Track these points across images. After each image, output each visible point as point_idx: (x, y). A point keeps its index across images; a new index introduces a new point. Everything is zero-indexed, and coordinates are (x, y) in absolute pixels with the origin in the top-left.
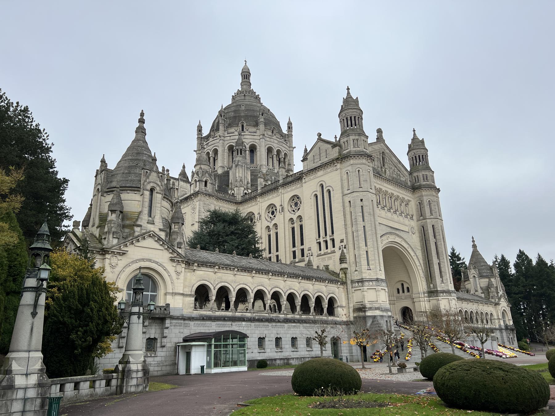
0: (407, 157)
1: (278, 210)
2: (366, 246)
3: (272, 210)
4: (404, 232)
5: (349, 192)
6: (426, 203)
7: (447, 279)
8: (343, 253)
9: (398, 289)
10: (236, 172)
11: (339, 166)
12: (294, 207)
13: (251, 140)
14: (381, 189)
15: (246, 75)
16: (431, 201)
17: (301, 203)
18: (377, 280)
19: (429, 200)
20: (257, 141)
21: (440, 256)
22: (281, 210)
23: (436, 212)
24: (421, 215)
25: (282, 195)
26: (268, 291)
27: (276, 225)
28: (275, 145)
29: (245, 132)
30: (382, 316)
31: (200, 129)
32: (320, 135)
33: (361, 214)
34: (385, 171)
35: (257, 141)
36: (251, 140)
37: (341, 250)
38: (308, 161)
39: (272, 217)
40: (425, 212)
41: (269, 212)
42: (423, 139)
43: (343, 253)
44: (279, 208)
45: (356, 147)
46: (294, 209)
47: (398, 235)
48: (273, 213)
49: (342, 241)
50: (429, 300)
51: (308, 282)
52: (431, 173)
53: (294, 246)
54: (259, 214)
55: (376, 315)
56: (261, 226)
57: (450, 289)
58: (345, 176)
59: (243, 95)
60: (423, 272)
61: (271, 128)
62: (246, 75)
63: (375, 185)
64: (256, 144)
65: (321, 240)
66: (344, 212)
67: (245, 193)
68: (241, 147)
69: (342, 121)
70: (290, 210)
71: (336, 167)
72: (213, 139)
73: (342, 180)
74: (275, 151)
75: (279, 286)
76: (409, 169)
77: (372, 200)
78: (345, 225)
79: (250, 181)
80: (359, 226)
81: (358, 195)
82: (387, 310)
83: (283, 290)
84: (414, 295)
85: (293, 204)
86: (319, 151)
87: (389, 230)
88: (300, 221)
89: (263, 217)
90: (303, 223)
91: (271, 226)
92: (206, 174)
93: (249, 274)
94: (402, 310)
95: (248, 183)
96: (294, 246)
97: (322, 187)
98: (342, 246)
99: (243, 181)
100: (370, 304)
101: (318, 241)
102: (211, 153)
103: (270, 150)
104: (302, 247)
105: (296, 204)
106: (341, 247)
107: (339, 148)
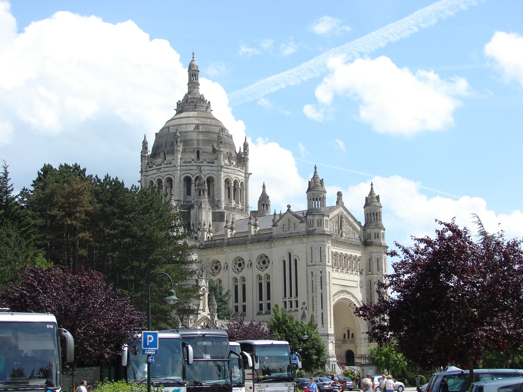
0: (363, 210)
1: (246, 265)
2: (322, 308)
3: (240, 263)
5: (312, 264)
6: (374, 260)
8: (304, 312)
9: (345, 335)
10: (199, 215)
11: (305, 240)
12: (262, 264)
13: (209, 172)
14: (337, 252)
16: (379, 259)
17: (269, 262)
18: (328, 335)
19: (378, 257)
20: (214, 172)
22: (249, 265)
23: (382, 269)
24: (370, 271)
25: (251, 252)
27: (244, 279)
28: (233, 176)
29: (202, 162)
31: (145, 143)
32: (289, 206)
33: (320, 284)
34: (342, 234)
35: (214, 172)
36: (209, 172)
37: (303, 310)
38: (278, 228)
39: (240, 269)
40: (373, 268)
41: (236, 264)
42: (379, 195)
43: (304, 312)
44: (246, 263)
46: (262, 266)
48: (240, 265)
49: (304, 303)
50: (369, 345)
52: (382, 231)
53: (261, 299)
54: (226, 263)
56: (228, 276)
58: (309, 250)
59: (194, 104)
61: (227, 154)
63: (333, 250)
64: (214, 176)
65: (287, 300)
66: (307, 281)
67: (208, 237)
68: (204, 188)
69: (309, 199)
70: (258, 267)
71: (303, 241)
72: (166, 166)
73: (307, 253)
74: (232, 182)
76: (363, 224)
77: (329, 272)
78: (308, 291)
79: (211, 223)
80: (317, 293)
81: (319, 267)
82: (333, 357)
84: (356, 341)
85: (262, 261)
86: (288, 221)
87: (341, 288)
88: (267, 278)
89: (230, 268)
90: (271, 281)
91: (238, 277)
94: (346, 353)
95: (210, 226)
96: (261, 299)
97: (290, 255)
98: (304, 307)
99: (206, 224)
101: (284, 300)
102: (163, 181)
103: (227, 181)
104: (269, 302)
105: (264, 262)
106: (303, 308)
107: (306, 224)
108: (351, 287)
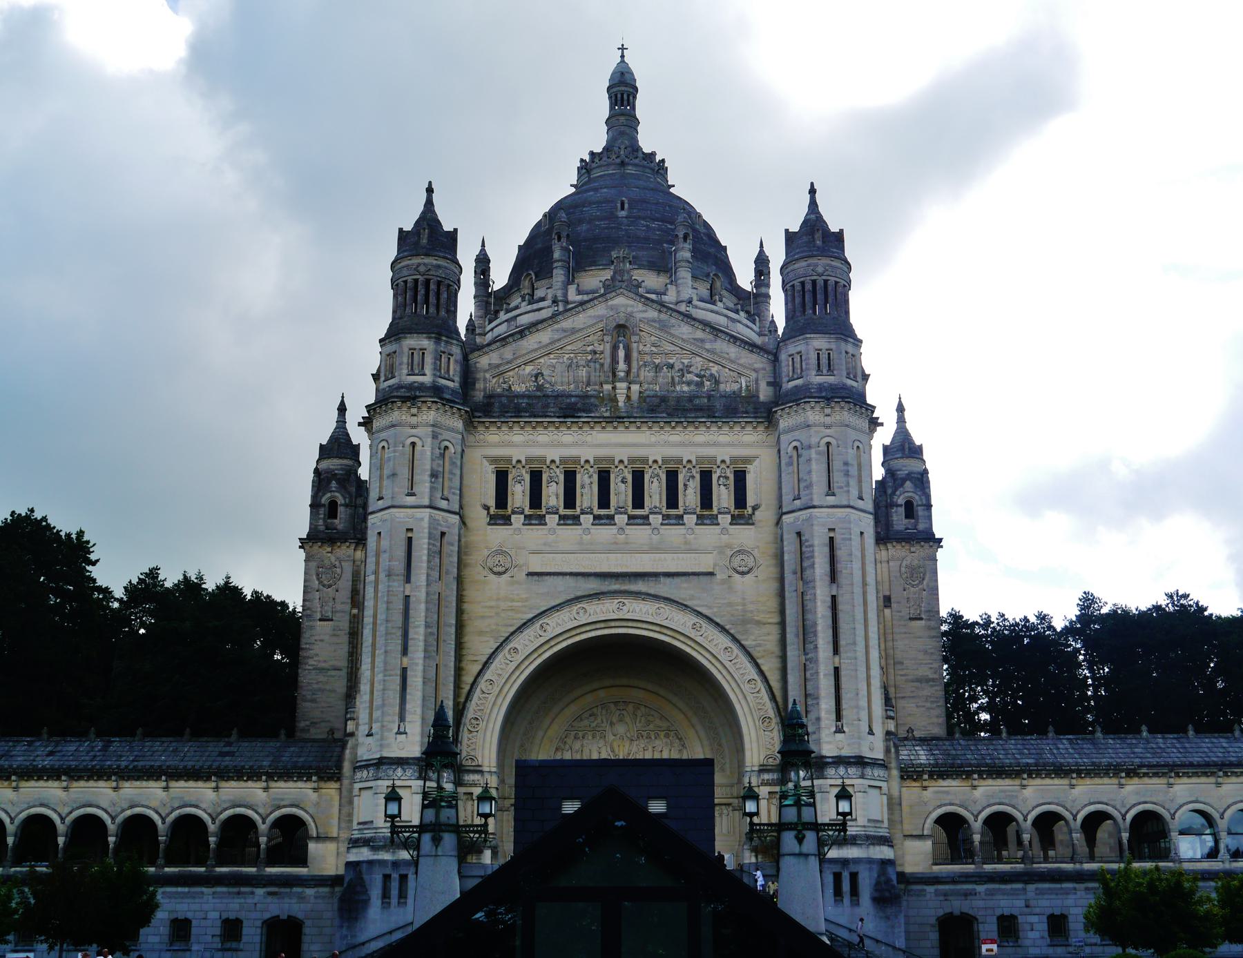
4: (677, 580)
7: (818, 719)
15: (622, 95)
19: (795, 444)
21: (810, 637)
23: (809, 486)
26: (60, 815)
30: (371, 863)
34: (614, 388)
45: (417, 372)
47: (637, 595)
51: (200, 784)
55: (361, 859)
57: (867, 754)
60: (773, 697)
62: (622, 95)
75: (94, 803)
83: (109, 810)
87: (593, 585)
92: (329, 482)
93: (6, 784)
100: (359, 830)
108: (662, 579)
